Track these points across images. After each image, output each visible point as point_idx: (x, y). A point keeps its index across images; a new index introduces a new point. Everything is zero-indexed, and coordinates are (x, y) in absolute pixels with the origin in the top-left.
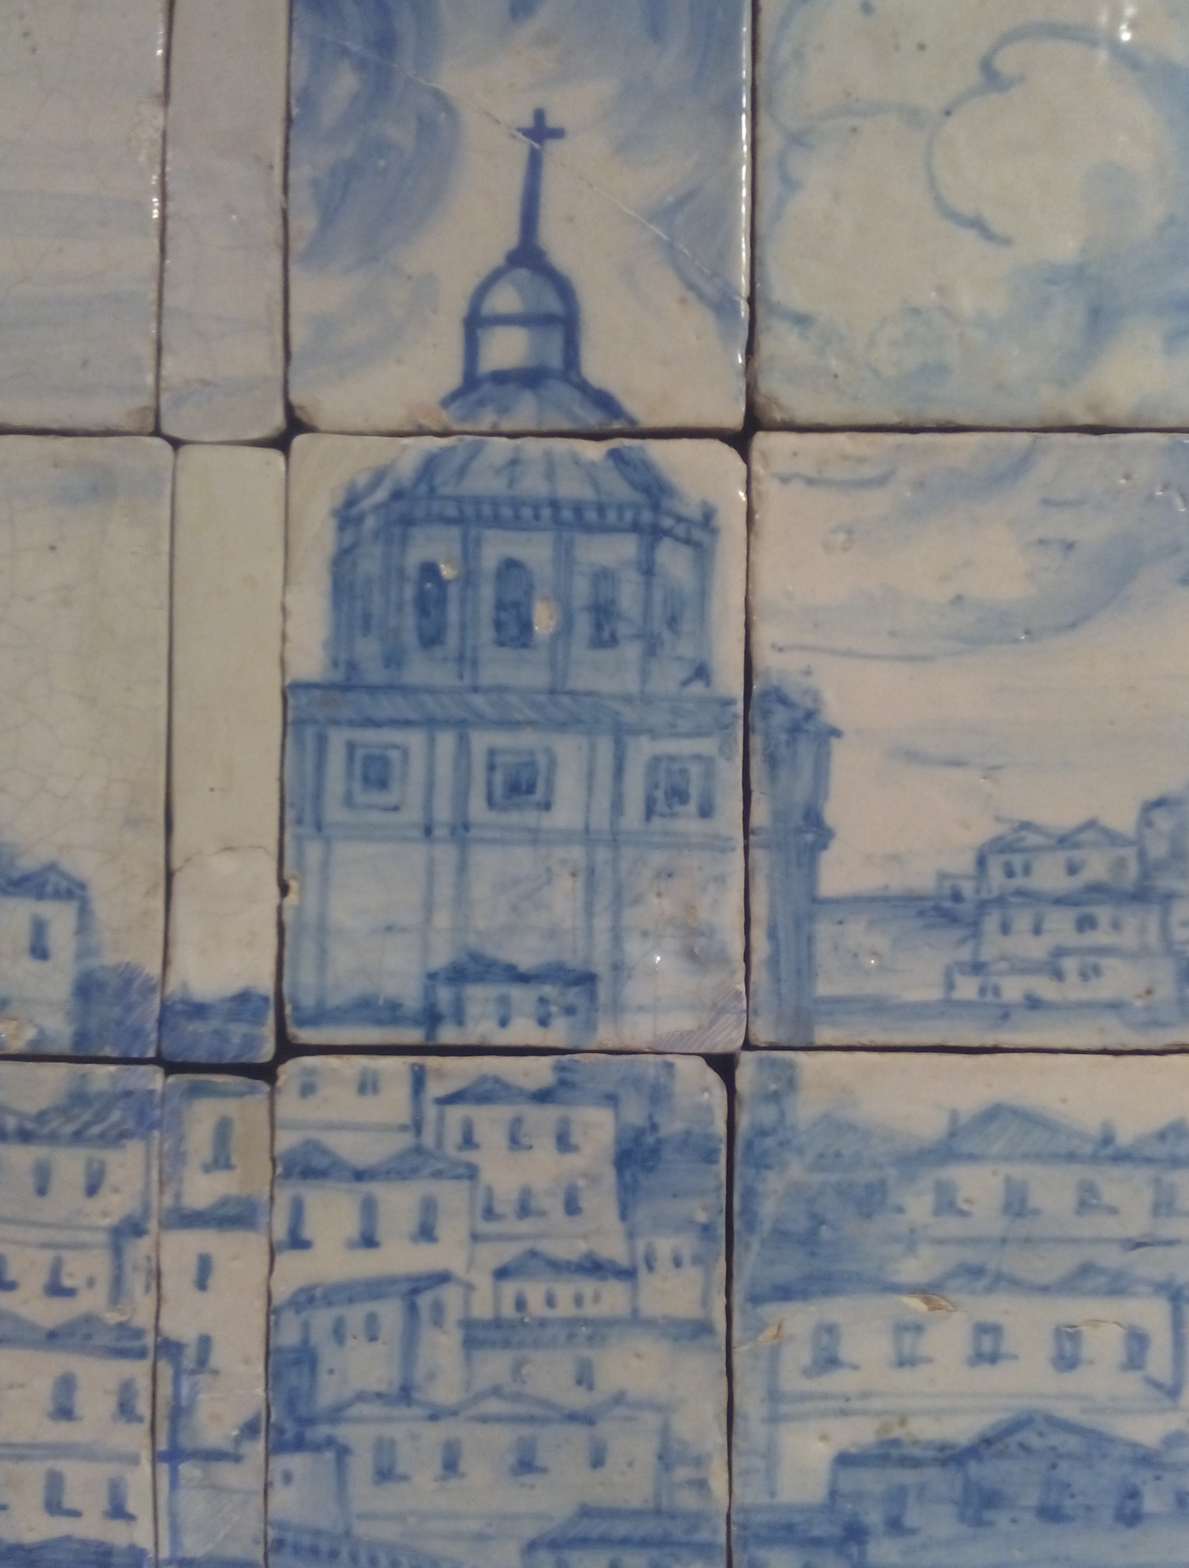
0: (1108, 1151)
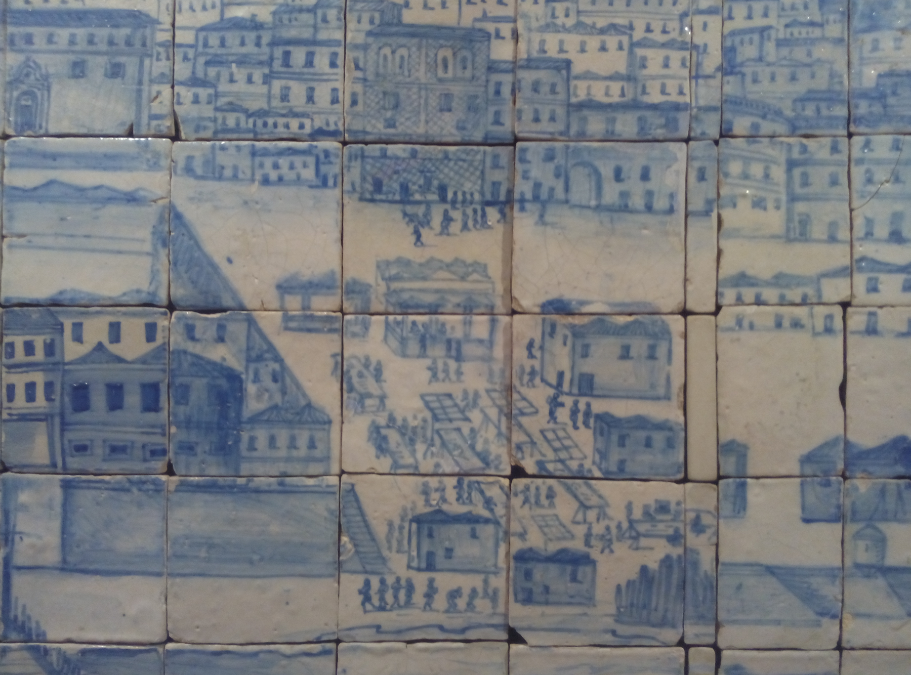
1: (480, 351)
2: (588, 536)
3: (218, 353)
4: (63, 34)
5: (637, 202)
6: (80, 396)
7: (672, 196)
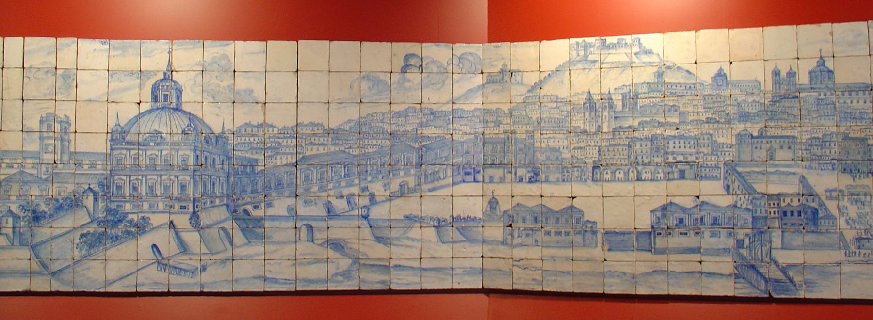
3: (813, 205)
4: (778, 140)
6: (785, 214)
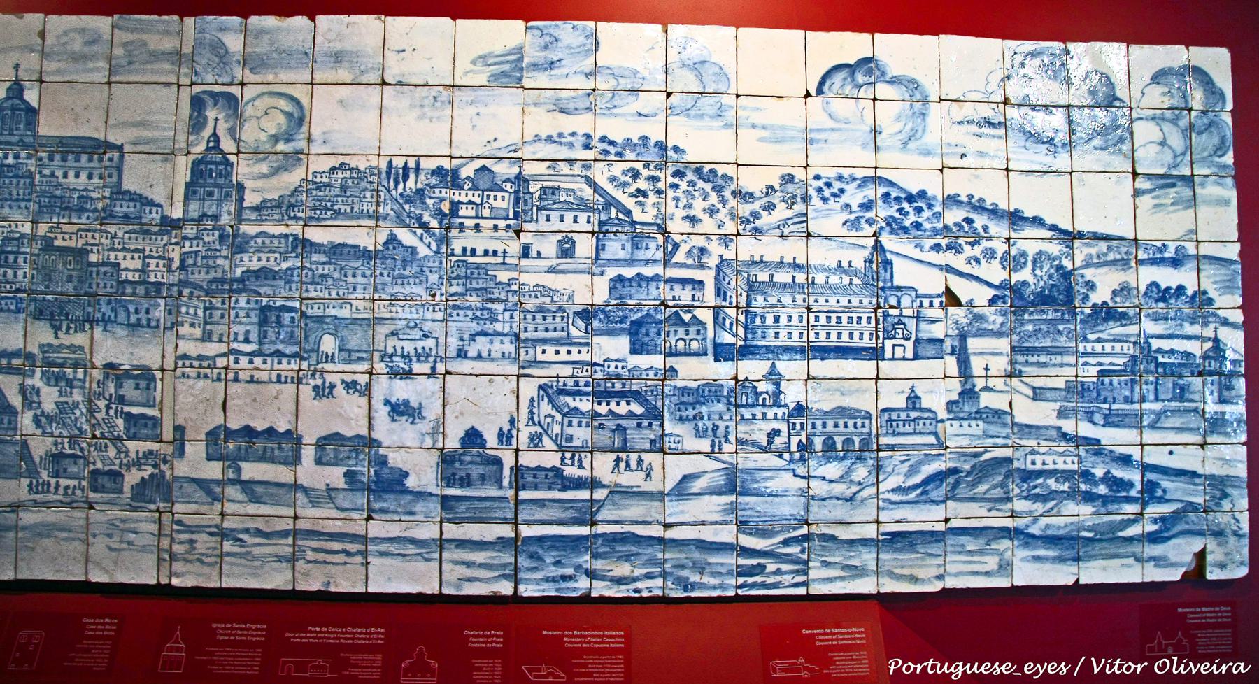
0: (274, 236)
1: (80, 384)
2: (121, 464)
5: (144, 322)
7: (158, 321)
